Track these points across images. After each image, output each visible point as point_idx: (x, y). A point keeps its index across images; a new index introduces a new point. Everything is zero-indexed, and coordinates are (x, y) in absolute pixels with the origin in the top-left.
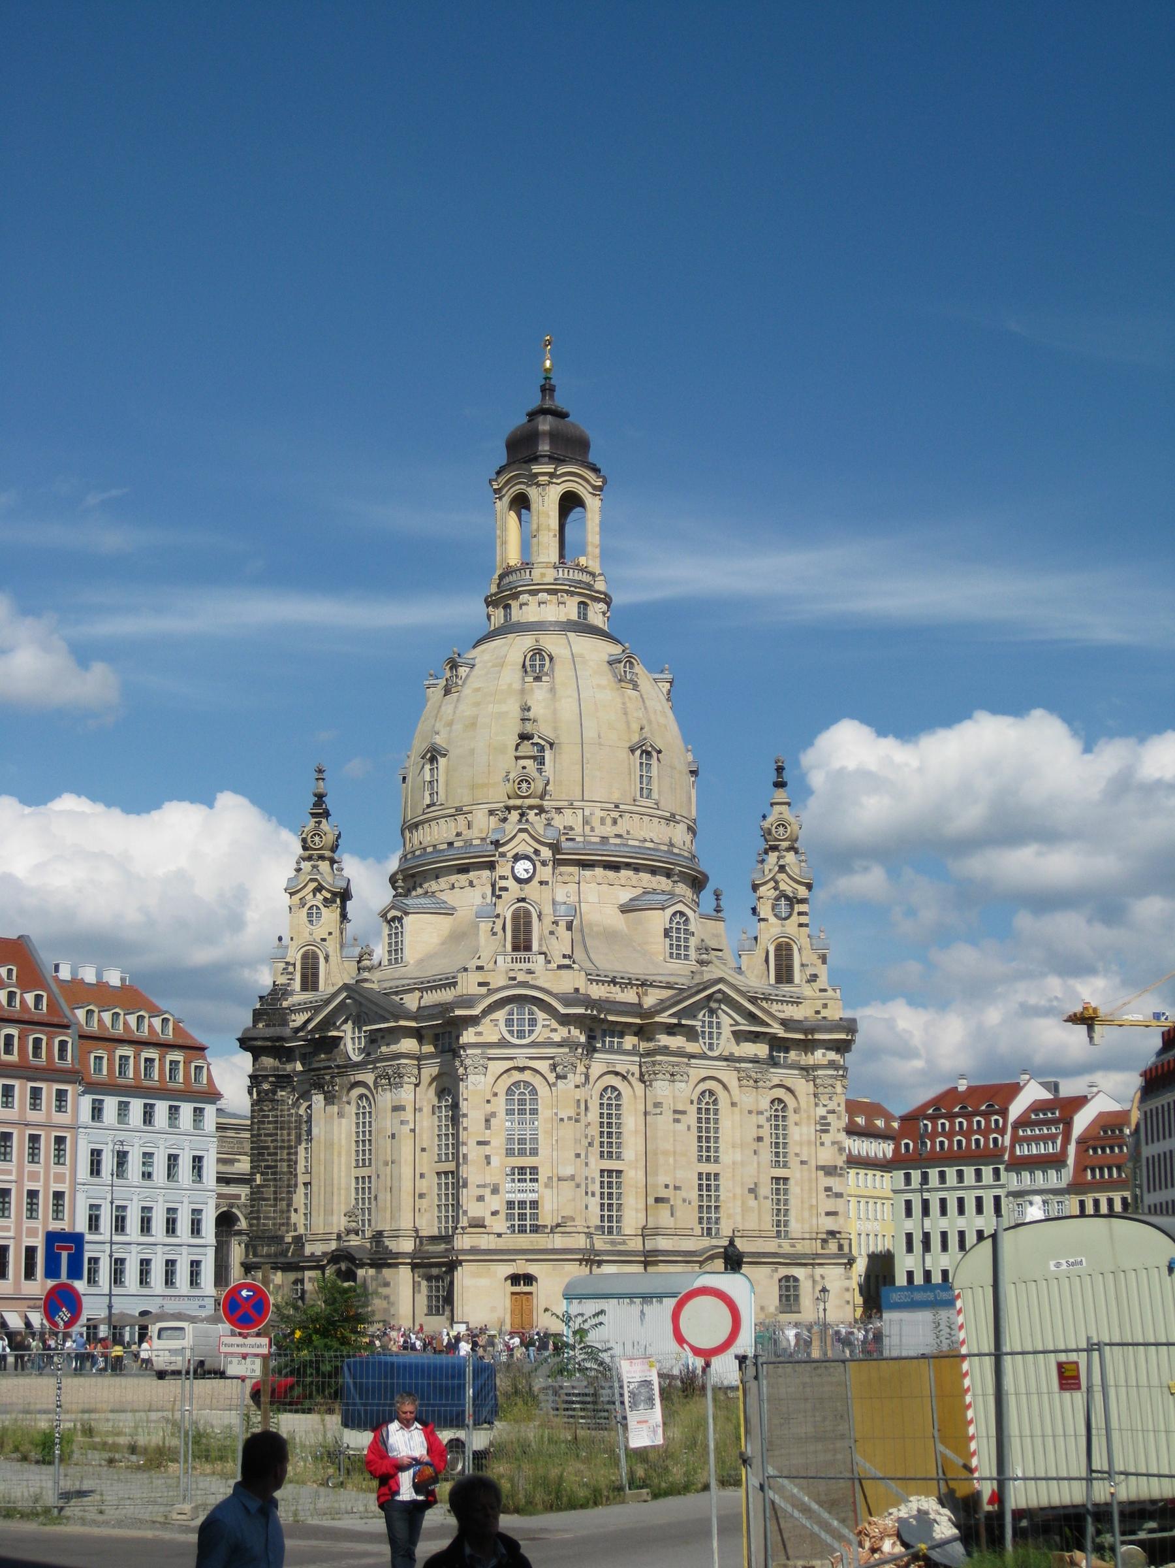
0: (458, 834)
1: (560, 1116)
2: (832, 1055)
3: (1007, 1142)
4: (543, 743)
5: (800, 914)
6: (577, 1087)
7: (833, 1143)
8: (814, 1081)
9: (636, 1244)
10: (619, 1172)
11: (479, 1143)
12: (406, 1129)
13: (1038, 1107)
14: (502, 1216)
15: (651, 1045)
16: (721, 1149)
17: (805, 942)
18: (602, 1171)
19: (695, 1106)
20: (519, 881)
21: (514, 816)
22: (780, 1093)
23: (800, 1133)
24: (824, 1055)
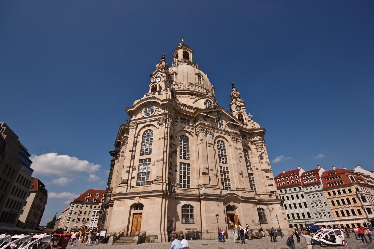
1: (159, 138)
2: (259, 137)
3: (301, 181)
4: (173, 73)
5: (243, 109)
6: (166, 128)
7: (266, 162)
8: (255, 145)
9: (196, 192)
10: (189, 165)
11: (130, 151)
13: (303, 173)
14: (136, 179)
16: (228, 160)
17: (246, 115)
24: (257, 138)
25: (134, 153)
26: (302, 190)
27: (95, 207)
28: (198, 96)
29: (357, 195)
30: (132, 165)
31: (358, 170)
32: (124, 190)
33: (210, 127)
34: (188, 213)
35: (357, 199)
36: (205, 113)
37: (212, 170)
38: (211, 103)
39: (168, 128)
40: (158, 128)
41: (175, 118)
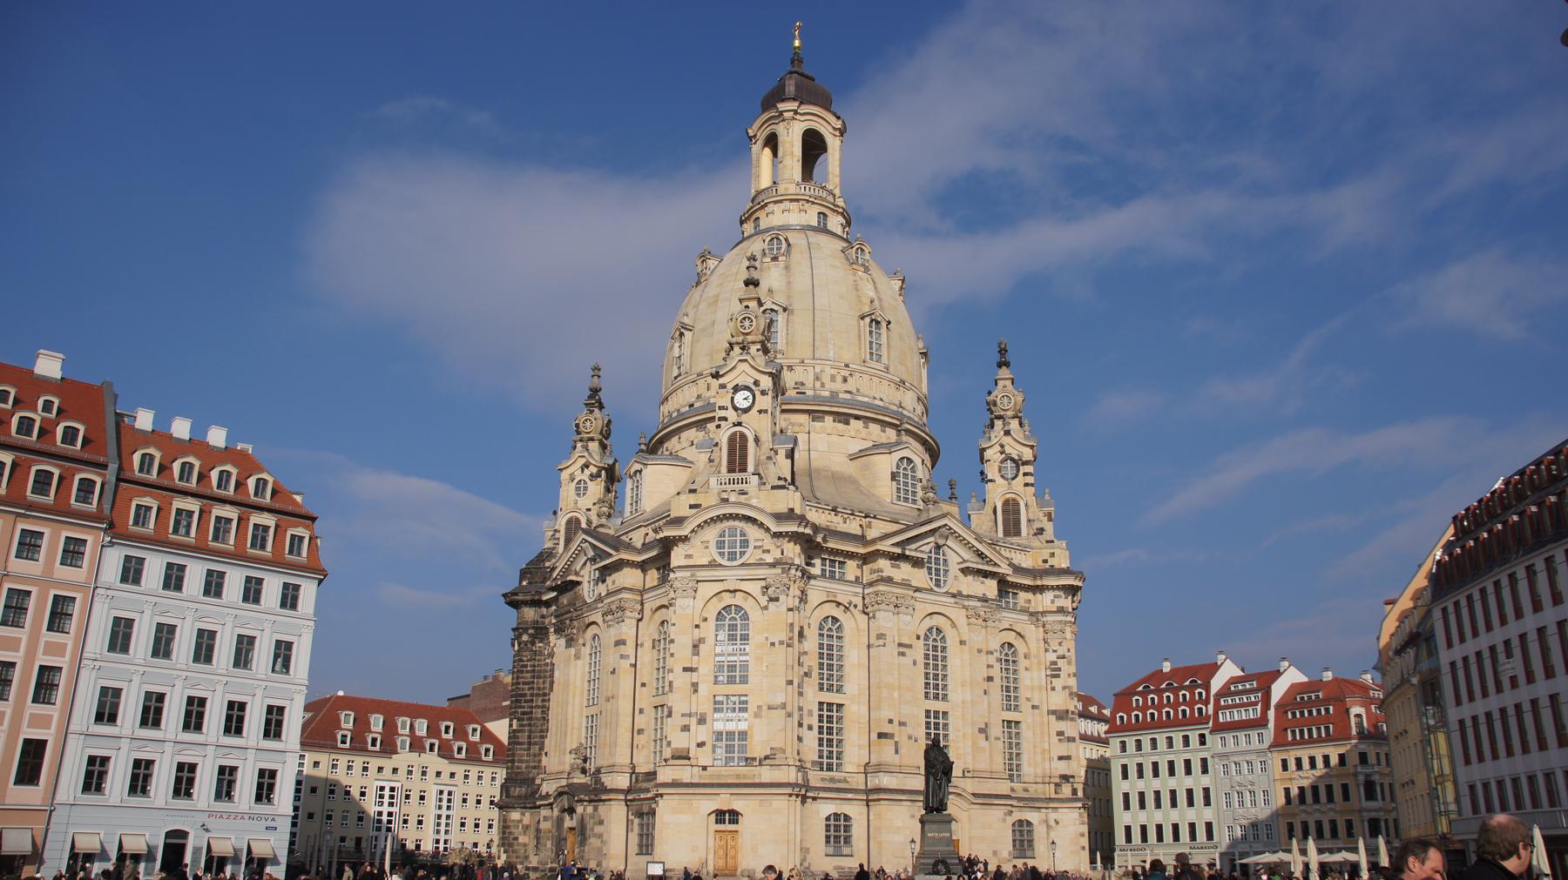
0: (699, 397)
3: (1211, 712)
6: (790, 610)
7: (1064, 688)
9: (858, 782)
10: (840, 706)
11: (685, 669)
12: (626, 664)
13: (1235, 680)
14: (708, 747)
15: (875, 577)
17: (1032, 501)
18: (821, 704)
19: (922, 642)
20: (736, 409)
21: (737, 349)
22: (1010, 637)
23: (1031, 679)
27: (380, 769)
29: (1355, 775)
34: (838, 832)
35: (1352, 789)
37: (901, 724)
38: (913, 470)
40: (766, 608)
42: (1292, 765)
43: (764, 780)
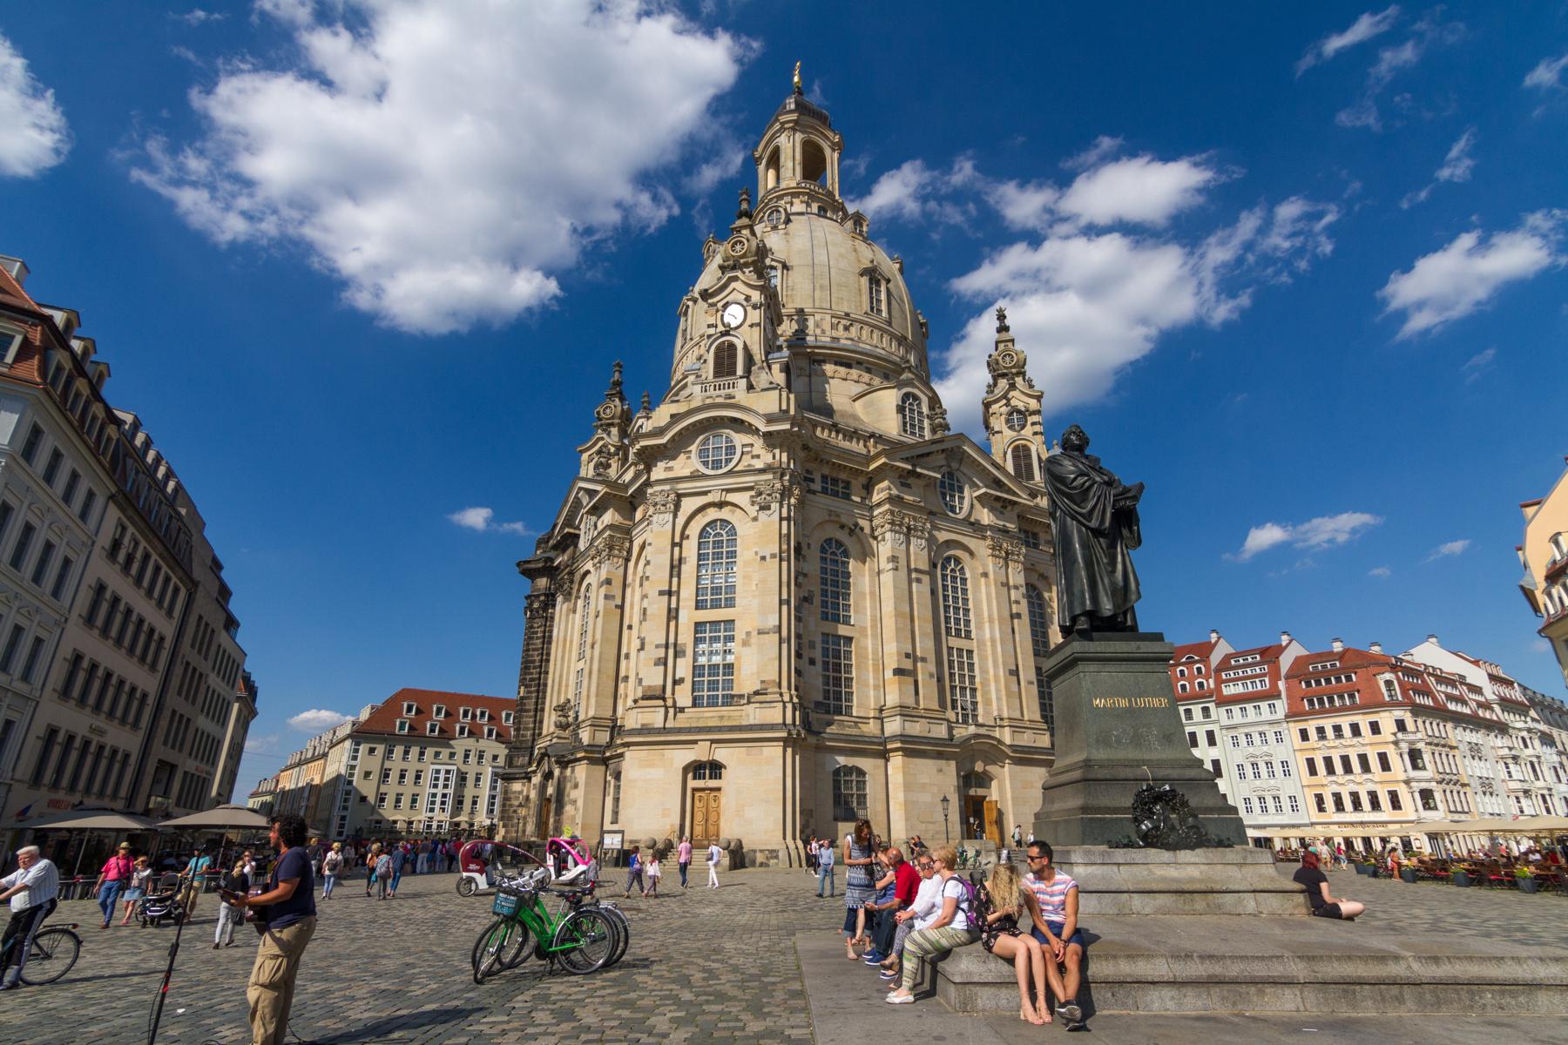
9: (871, 728)
10: (850, 639)
11: (661, 593)
12: (612, 604)
13: (1228, 657)
14: (688, 685)
15: (883, 495)
16: (973, 624)
25: (674, 599)
26: (1214, 716)
28: (869, 371)
30: (672, 640)
31: (1429, 654)
32: (656, 718)
33: (920, 509)
36: (906, 460)
39: (788, 519)
40: (755, 519)
41: (806, 479)
42: (1313, 734)
43: (752, 722)
